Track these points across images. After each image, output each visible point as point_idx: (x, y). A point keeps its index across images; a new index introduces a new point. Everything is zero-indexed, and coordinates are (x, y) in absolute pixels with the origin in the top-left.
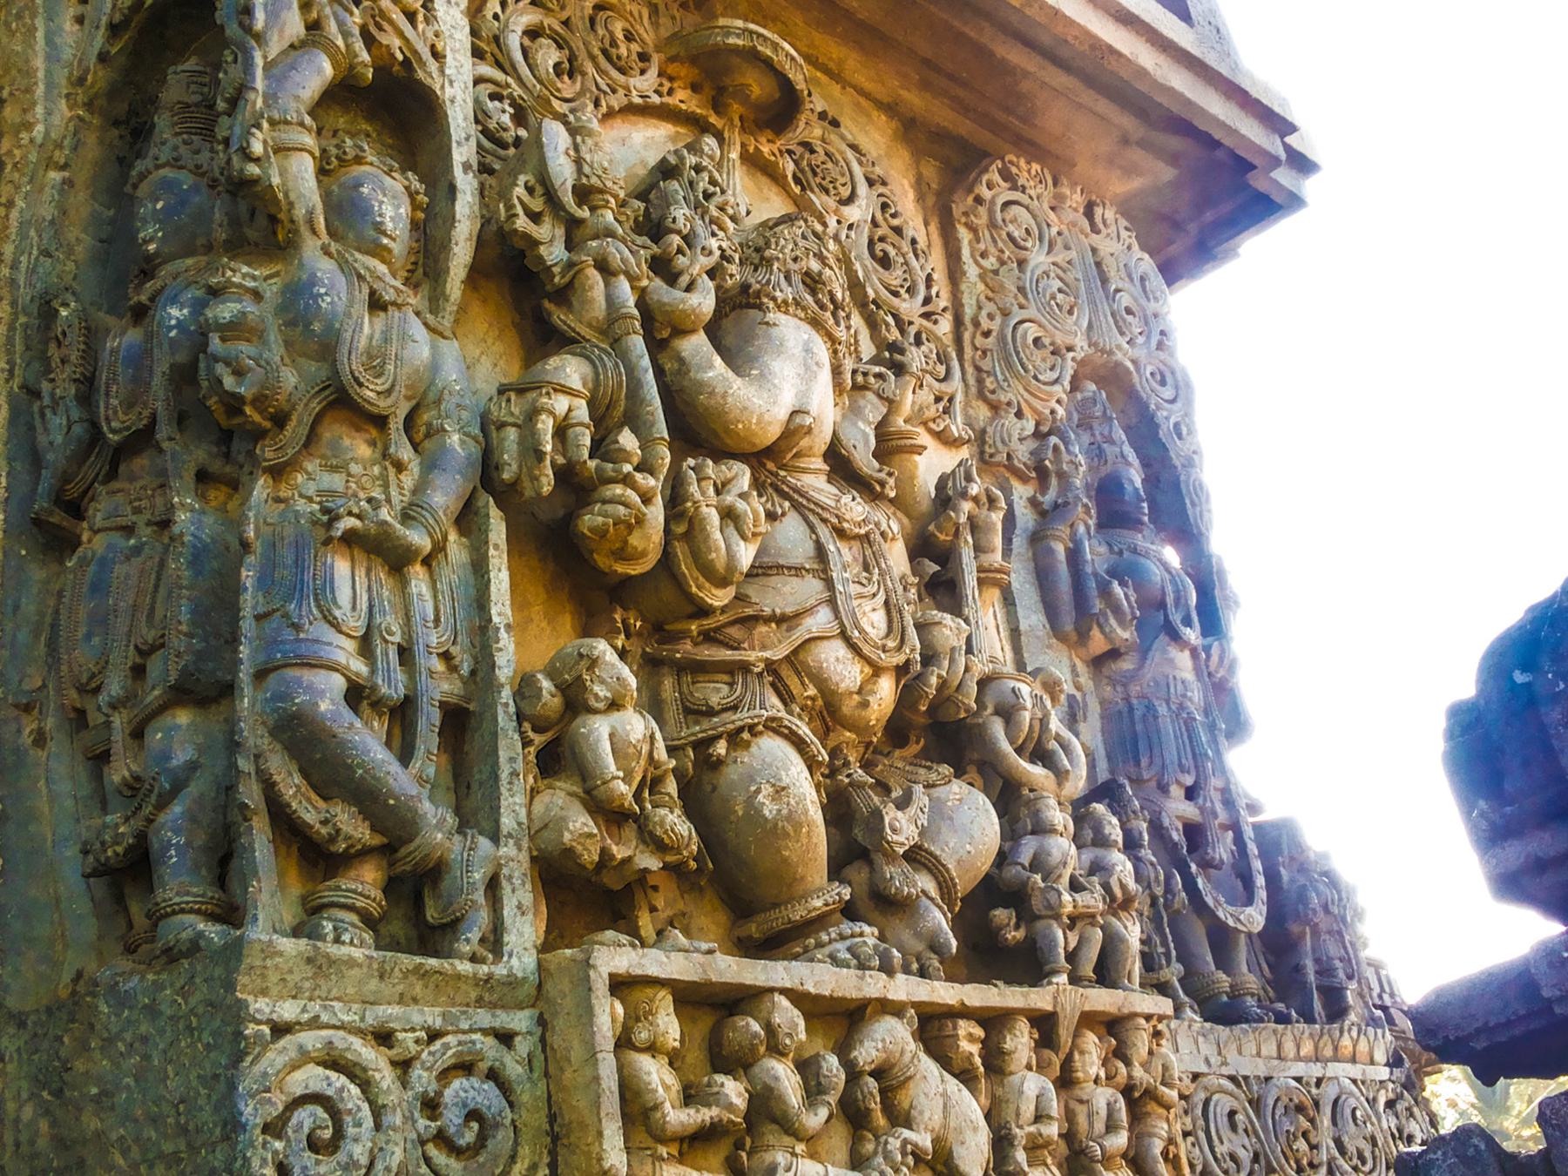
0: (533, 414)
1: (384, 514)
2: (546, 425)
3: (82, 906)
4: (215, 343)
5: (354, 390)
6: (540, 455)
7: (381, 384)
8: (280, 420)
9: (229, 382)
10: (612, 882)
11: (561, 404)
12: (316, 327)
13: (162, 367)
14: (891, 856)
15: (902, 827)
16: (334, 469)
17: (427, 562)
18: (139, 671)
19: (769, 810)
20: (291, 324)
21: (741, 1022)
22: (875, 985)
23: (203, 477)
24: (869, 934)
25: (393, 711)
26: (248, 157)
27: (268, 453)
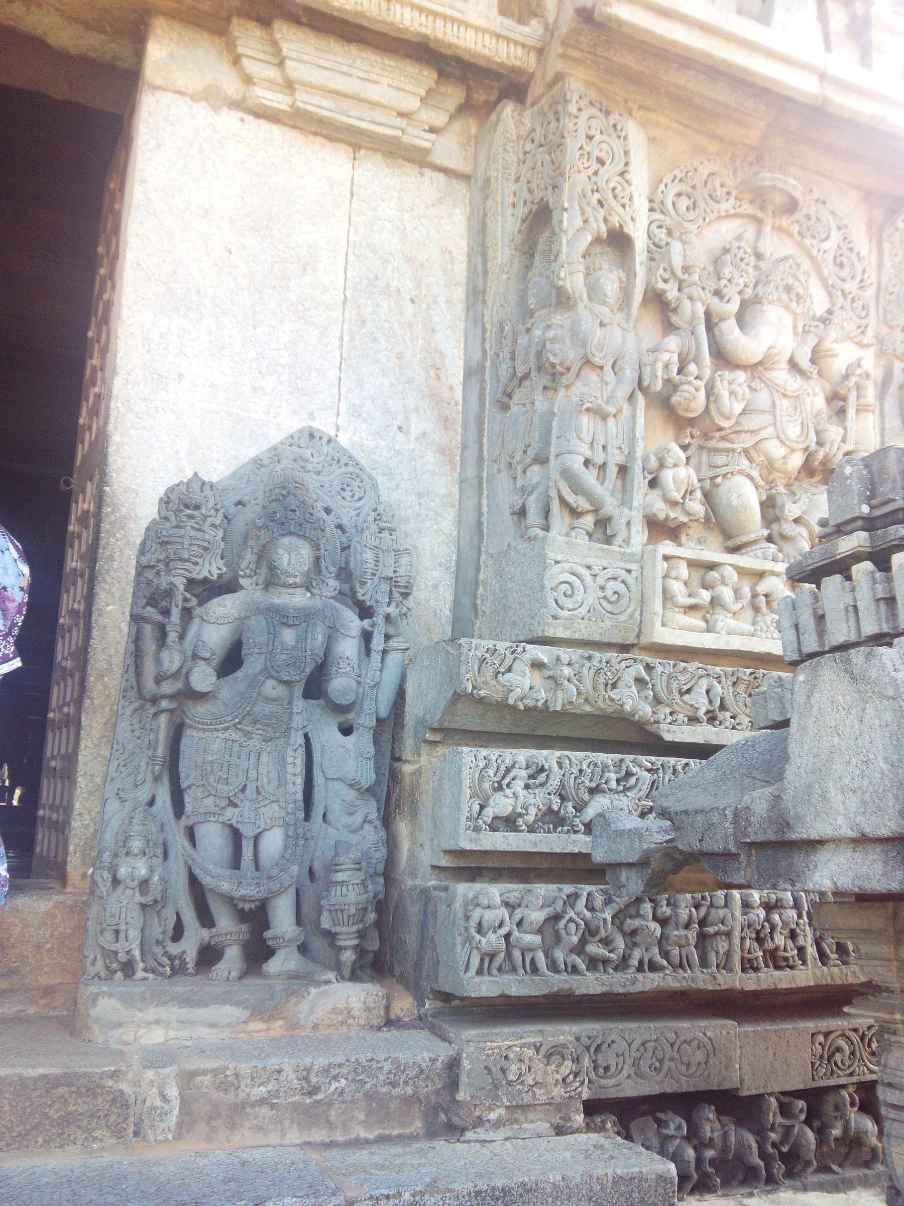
0: (655, 361)
1: (600, 402)
2: (659, 366)
3: (511, 523)
4: (548, 345)
5: (592, 359)
6: (656, 377)
7: (602, 355)
8: (568, 369)
9: (552, 359)
10: (672, 525)
11: (666, 357)
12: (581, 336)
13: (533, 352)
14: (786, 521)
15: (792, 510)
16: (585, 385)
17: (615, 416)
18: (525, 452)
19: (735, 502)
20: (573, 336)
21: (711, 573)
22: (769, 566)
23: (545, 388)
24: (772, 548)
25: (600, 467)
26: (559, 279)
27: (564, 381)
